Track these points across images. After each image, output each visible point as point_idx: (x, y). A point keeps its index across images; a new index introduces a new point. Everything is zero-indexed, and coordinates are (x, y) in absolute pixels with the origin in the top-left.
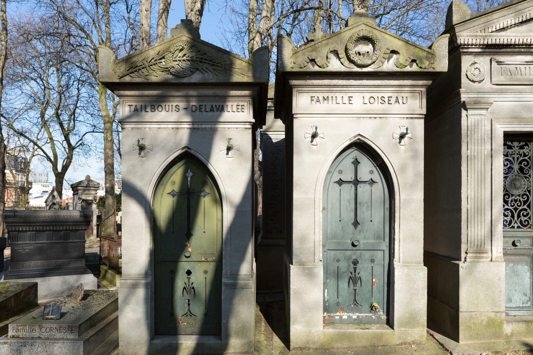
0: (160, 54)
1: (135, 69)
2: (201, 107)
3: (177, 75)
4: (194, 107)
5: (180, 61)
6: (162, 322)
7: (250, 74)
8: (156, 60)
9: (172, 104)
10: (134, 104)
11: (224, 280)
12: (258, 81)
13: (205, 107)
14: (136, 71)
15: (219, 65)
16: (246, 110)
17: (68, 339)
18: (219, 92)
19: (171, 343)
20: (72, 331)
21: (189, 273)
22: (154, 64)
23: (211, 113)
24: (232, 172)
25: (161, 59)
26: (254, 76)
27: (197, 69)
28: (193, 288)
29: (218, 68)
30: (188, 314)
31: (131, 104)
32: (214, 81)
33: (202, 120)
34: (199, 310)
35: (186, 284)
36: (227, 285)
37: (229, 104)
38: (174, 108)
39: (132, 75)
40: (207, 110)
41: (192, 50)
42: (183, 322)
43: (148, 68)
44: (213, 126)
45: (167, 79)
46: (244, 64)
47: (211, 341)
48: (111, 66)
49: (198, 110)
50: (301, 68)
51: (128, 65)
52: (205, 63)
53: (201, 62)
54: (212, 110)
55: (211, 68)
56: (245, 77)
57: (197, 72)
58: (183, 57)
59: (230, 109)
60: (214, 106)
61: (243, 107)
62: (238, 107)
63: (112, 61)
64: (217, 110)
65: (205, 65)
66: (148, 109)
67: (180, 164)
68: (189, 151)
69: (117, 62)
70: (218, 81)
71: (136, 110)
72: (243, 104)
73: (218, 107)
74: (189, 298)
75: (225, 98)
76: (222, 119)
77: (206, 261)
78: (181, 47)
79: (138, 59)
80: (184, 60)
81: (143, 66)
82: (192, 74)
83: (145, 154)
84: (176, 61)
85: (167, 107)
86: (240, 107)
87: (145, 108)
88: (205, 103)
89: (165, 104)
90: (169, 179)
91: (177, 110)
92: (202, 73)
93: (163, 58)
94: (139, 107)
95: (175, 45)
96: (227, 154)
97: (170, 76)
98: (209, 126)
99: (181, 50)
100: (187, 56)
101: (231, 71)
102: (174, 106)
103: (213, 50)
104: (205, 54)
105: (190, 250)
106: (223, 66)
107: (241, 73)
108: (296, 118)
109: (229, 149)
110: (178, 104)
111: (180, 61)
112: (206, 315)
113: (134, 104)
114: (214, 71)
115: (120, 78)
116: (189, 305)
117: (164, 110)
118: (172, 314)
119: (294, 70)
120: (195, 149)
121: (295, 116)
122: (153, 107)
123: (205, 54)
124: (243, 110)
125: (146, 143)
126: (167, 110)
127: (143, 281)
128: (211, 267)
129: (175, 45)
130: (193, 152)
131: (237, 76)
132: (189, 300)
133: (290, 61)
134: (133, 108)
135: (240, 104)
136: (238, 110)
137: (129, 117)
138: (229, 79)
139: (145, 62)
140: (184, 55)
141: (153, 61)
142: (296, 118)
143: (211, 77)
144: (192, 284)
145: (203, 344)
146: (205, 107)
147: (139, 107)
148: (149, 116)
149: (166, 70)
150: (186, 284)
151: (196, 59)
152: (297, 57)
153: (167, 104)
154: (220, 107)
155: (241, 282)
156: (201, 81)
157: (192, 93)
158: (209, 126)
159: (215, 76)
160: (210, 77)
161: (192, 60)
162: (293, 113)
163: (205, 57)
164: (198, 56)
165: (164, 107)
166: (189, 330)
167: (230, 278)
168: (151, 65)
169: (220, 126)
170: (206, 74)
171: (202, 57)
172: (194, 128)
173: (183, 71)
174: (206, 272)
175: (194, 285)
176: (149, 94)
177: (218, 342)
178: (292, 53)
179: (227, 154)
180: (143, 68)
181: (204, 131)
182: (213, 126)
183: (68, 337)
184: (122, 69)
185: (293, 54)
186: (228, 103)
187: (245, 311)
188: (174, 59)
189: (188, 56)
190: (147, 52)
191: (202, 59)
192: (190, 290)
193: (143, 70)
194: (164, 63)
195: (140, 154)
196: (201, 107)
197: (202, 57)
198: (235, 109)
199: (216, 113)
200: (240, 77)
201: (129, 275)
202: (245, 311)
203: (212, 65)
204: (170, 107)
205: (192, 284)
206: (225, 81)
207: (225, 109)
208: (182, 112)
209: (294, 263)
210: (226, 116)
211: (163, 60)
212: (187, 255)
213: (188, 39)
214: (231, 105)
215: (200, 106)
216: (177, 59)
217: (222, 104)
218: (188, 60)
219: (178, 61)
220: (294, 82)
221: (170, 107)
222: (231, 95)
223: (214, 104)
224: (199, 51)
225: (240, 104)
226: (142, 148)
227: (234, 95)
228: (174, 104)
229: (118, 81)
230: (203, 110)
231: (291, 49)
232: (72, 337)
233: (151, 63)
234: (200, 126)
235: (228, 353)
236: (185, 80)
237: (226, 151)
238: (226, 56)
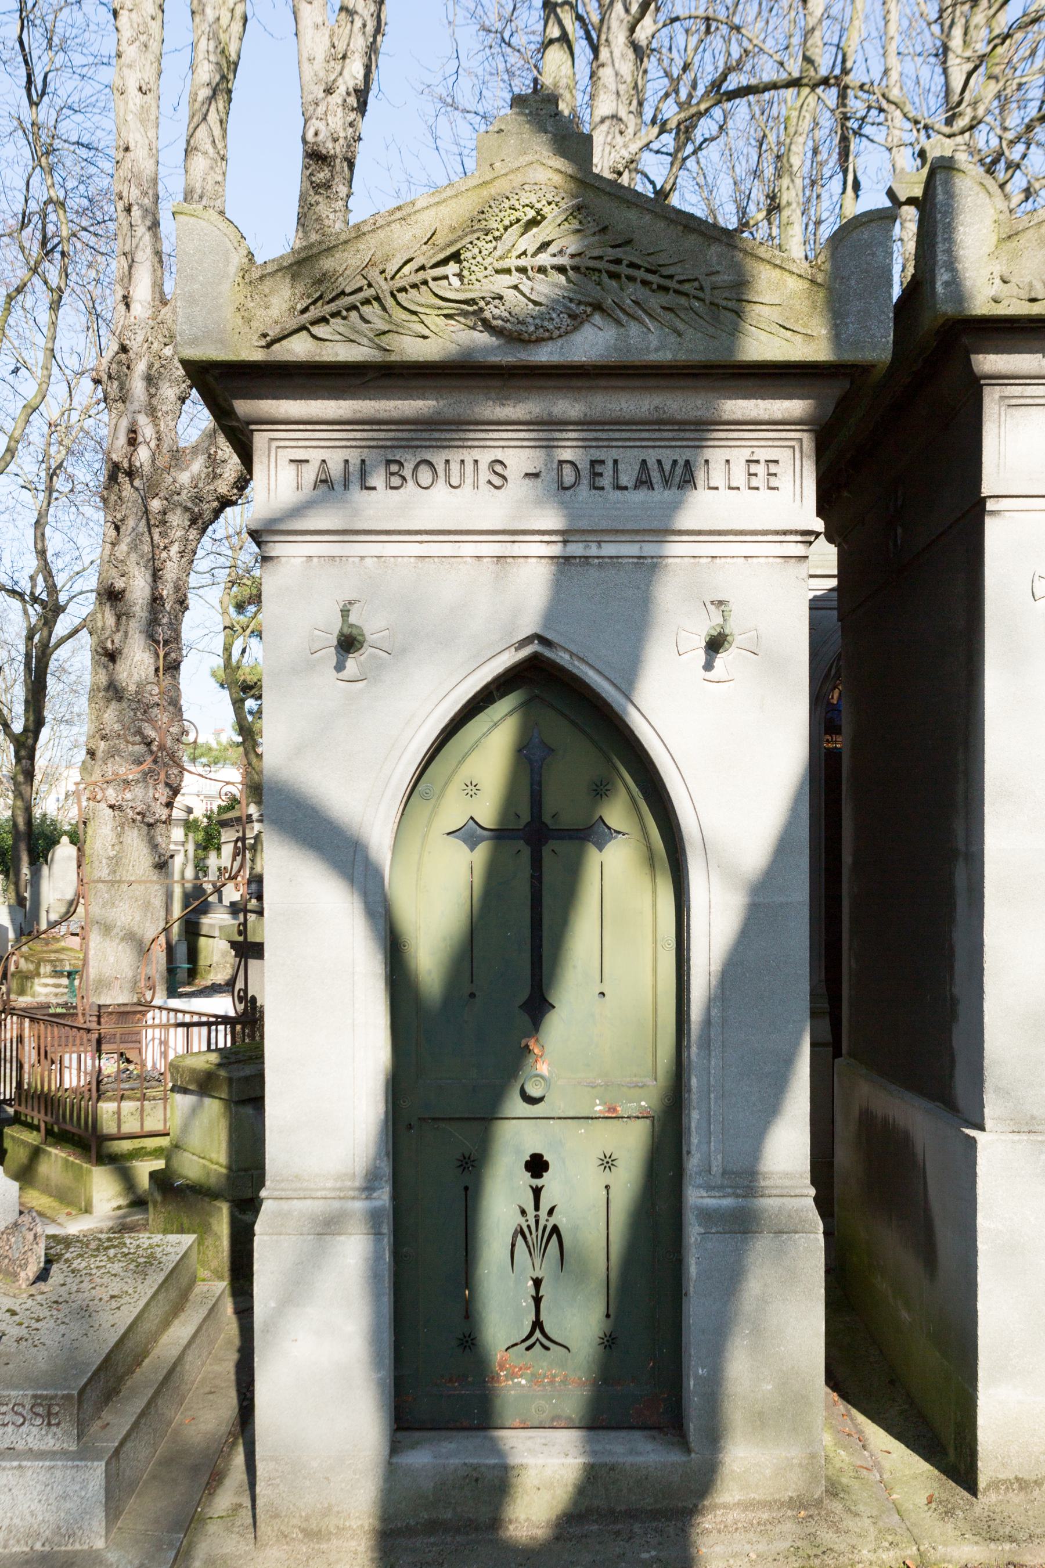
0: (440, 240)
1: (332, 307)
2: (599, 469)
3: (512, 334)
4: (567, 469)
5: (522, 270)
6: (434, 1374)
7: (820, 329)
8: (423, 268)
9: (476, 454)
10: (315, 456)
11: (695, 1197)
12: (849, 357)
13: (616, 471)
14: (335, 314)
15: (686, 287)
16: (785, 479)
17: (41, 1455)
18: (678, 404)
19: (476, 1468)
20: (49, 1419)
21: (537, 1165)
22: (414, 286)
23: (641, 496)
24: (733, 738)
25: (444, 262)
26: (837, 337)
27: (598, 307)
28: (555, 1229)
29: (683, 301)
30: (539, 1336)
31: (300, 455)
32: (665, 356)
33: (604, 525)
34: (580, 1322)
35: (523, 1212)
36: (707, 1216)
37: (716, 456)
38: (485, 474)
39: (319, 330)
40: (624, 480)
41: (575, 225)
42: (512, 1376)
43: (389, 302)
44: (649, 549)
45: (469, 351)
46: (794, 284)
47: (643, 1454)
48: (229, 292)
49: (585, 482)
50: (1033, 300)
51: (300, 289)
52: (631, 279)
53: (613, 275)
54: (643, 481)
55: (655, 301)
56: (798, 338)
57: (597, 318)
58: (534, 255)
59: (717, 478)
60: (652, 464)
61: (773, 468)
62: (754, 468)
63: (232, 269)
64: (667, 482)
65: (631, 288)
66: (378, 479)
67: (503, 706)
68: (548, 653)
69: (256, 274)
70: (682, 357)
71: (324, 482)
72: (772, 454)
73: (667, 468)
74: (538, 1274)
75: (700, 429)
76: (686, 520)
77: (612, 1116)
78: (531, 214)
79: (346, 265)
80: (542, 270)
81: (368, 293)
82: (576, 328)
83: (360, 665)
84: (508, 271)
85: (455, 467)
86: (760, 469)
87: (363, 474)
88: (614, 454)
89: (445, 454)
90: (454, 772)
91: (497, 481)
92: (618, 322)
93: (456, 257)
94: (335, 469)
95: (507, 204)
96: (708, 666)
97: (482, 338)
98: (632, 550)
99: (534, 223)
100: (553, 249)
101: (739, 314)
102: (483, 466)
103: (662, 224)
104: (629, 242)
105: (543, 1068)
106: (707, 295)
107: (785, 321)
108: (992, 512)
109: (715, 645)
110: (499, 454)
111: (522, 270)
112: (609, 1342)
113: (315, 456)
114: (670, 316)
115: (269, 346)
116: (537, 1300)
117: (410, 483)
118: (468, 1340)
119: (1001, 310)
120: (573, 648)
121: (990, 505)
122: (394, 468)
123: (629, 242)
124: (774, 481)
125: (371, 623)
126: (455, 481)
127: (359, 1206)
128: (630, 1143)
129: (507, 204)
130: (562, 658)
131: (763, 336)
132: (537, 1283)
133: (985, 273)
134: (310, 474)
135: (762, 454)
136: (754, 482)
137: (298, 511)
138: (731, 349)
139: (373, 274)
140: (544, 246)
141: (406, 270)
142: (992, 512)
143: (654, 340)
144: (551, 1212)
145: (612, 1468)
146: (616, 471)
147: (335, 469)
148: (381, 504)
149: (471, 310)
150: (523, 1212)
151: (592, 264)
152: (1015, 256)
153: (455, 456)
154: (679, 470)
155: (768, 1204)
156: (614, 358)
157: (567, 406)
158: (632, 550)
159: (673, 338)
160: (651, 342)
161: (580, 270)
162: (985, 491)
163: (628, 255)
164: (596, 253)
165: (440, 468)
166: (541, 1407)
167: (721, 1187)
168: (403, 290)
169: (676, 548)
170: (634, 329)
171: (618, 253)
172: (567, 558)
173: (541, 316)
174: (608, 1163)
175: (559, 1219)
176: (383, 415)
177: (675, 1457)
178: (994, 239)
179: (708, 666)
180: (367, 302)
181: (609, 567)
182: (649, 549)
183: (34, 1444)
184: (281, 302)
185: (1002, 241)
186: (708, 454)
187: (777, 1325)
188: (499, 265)
189: (561, 252)
190: (381, 234)
191: (618, 262)
192: (546, 1236)
193: (365, 310)
194: (455, 281)
195: (340, 667)
196: (599, 469)
197: (618, 253)
198: (739, 477)
199: (660, 495)
200: (777, 342)
201: (298, 1178)
202: (777, 1325)
203: (665, 289)
204: (469, 467)
205: (551, 1212)
206: (714, 357)
207: (700, 476)
208: (517, 488)
209: (988, 1123)
210: (702, 507)
211: (452, 268)
212: (534, 1091)
213: (557, 179)
214: (724, 461)
215: (593, 463)
216: (512, 262)
217: (687, 454)
218: (561, 269)
219: (523, 269)
220: (989, 363)
221: (469, 467)
222: (726, 417)
223: (652, 457)
224: (604, 230)
225: (762, 454)
226: (348, 643)
227: (738, 416)
228: (485, 457)
229: (258, 356)
230: (606, 481)
231: (989, 222)
232: (50, 1443)
233: (399, 283)
234: (593, 550)
235: (715, 1507)
236: (545, 355)
237: (701, 656)
238: (714, 251)
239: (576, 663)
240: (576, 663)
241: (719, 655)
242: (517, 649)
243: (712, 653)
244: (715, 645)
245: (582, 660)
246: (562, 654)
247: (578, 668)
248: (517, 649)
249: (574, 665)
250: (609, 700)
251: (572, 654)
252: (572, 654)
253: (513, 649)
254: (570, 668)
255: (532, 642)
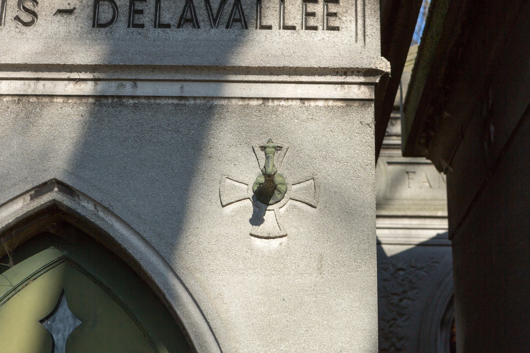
23: (186, 33)
33: (138, 61)
40: (166, 17)
49: (123, 19)
64: (214, 21)
91: (26, 18)
96: (257, 219)
98: (174, 89)
109: (265, 194)
120: (97, 196)
124: (334, 22)
130: (85, 208)
136: (312, 22)
158: (174, 89)
179: (257, 219)
230: (147, 19)
234: (128, 89)
239: (101, 214)
240: (101, 214)
241: (270, 207)
242: (32, 198)
243: (261, 204)
244: (265, 194)
245: (106, 209)
246: (84, 203)
247: (103, 220)
248: (32, 198)
249: (98, 217)
250: (137, 257)
251: (96, 203)
252: (96, 203)
253: (28, 197)
254: (93, 219)
255: (51, 190)
